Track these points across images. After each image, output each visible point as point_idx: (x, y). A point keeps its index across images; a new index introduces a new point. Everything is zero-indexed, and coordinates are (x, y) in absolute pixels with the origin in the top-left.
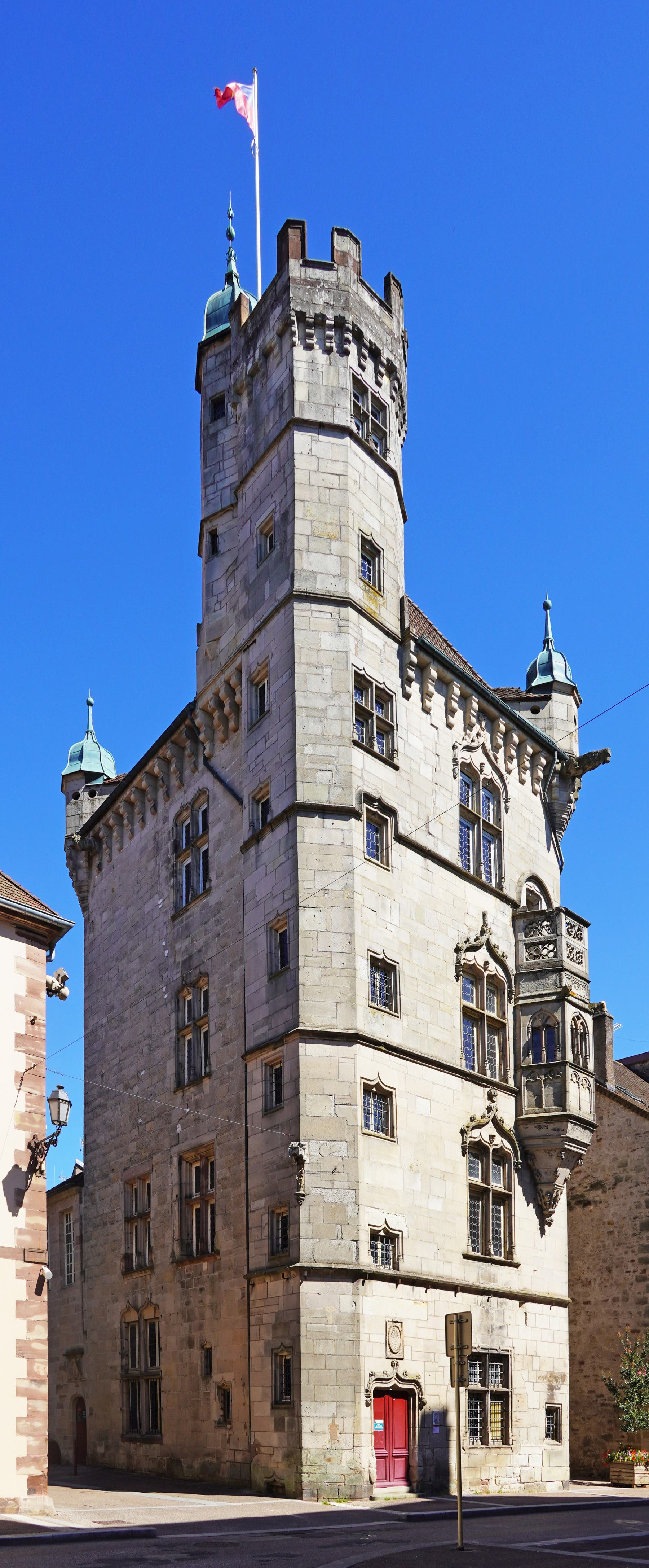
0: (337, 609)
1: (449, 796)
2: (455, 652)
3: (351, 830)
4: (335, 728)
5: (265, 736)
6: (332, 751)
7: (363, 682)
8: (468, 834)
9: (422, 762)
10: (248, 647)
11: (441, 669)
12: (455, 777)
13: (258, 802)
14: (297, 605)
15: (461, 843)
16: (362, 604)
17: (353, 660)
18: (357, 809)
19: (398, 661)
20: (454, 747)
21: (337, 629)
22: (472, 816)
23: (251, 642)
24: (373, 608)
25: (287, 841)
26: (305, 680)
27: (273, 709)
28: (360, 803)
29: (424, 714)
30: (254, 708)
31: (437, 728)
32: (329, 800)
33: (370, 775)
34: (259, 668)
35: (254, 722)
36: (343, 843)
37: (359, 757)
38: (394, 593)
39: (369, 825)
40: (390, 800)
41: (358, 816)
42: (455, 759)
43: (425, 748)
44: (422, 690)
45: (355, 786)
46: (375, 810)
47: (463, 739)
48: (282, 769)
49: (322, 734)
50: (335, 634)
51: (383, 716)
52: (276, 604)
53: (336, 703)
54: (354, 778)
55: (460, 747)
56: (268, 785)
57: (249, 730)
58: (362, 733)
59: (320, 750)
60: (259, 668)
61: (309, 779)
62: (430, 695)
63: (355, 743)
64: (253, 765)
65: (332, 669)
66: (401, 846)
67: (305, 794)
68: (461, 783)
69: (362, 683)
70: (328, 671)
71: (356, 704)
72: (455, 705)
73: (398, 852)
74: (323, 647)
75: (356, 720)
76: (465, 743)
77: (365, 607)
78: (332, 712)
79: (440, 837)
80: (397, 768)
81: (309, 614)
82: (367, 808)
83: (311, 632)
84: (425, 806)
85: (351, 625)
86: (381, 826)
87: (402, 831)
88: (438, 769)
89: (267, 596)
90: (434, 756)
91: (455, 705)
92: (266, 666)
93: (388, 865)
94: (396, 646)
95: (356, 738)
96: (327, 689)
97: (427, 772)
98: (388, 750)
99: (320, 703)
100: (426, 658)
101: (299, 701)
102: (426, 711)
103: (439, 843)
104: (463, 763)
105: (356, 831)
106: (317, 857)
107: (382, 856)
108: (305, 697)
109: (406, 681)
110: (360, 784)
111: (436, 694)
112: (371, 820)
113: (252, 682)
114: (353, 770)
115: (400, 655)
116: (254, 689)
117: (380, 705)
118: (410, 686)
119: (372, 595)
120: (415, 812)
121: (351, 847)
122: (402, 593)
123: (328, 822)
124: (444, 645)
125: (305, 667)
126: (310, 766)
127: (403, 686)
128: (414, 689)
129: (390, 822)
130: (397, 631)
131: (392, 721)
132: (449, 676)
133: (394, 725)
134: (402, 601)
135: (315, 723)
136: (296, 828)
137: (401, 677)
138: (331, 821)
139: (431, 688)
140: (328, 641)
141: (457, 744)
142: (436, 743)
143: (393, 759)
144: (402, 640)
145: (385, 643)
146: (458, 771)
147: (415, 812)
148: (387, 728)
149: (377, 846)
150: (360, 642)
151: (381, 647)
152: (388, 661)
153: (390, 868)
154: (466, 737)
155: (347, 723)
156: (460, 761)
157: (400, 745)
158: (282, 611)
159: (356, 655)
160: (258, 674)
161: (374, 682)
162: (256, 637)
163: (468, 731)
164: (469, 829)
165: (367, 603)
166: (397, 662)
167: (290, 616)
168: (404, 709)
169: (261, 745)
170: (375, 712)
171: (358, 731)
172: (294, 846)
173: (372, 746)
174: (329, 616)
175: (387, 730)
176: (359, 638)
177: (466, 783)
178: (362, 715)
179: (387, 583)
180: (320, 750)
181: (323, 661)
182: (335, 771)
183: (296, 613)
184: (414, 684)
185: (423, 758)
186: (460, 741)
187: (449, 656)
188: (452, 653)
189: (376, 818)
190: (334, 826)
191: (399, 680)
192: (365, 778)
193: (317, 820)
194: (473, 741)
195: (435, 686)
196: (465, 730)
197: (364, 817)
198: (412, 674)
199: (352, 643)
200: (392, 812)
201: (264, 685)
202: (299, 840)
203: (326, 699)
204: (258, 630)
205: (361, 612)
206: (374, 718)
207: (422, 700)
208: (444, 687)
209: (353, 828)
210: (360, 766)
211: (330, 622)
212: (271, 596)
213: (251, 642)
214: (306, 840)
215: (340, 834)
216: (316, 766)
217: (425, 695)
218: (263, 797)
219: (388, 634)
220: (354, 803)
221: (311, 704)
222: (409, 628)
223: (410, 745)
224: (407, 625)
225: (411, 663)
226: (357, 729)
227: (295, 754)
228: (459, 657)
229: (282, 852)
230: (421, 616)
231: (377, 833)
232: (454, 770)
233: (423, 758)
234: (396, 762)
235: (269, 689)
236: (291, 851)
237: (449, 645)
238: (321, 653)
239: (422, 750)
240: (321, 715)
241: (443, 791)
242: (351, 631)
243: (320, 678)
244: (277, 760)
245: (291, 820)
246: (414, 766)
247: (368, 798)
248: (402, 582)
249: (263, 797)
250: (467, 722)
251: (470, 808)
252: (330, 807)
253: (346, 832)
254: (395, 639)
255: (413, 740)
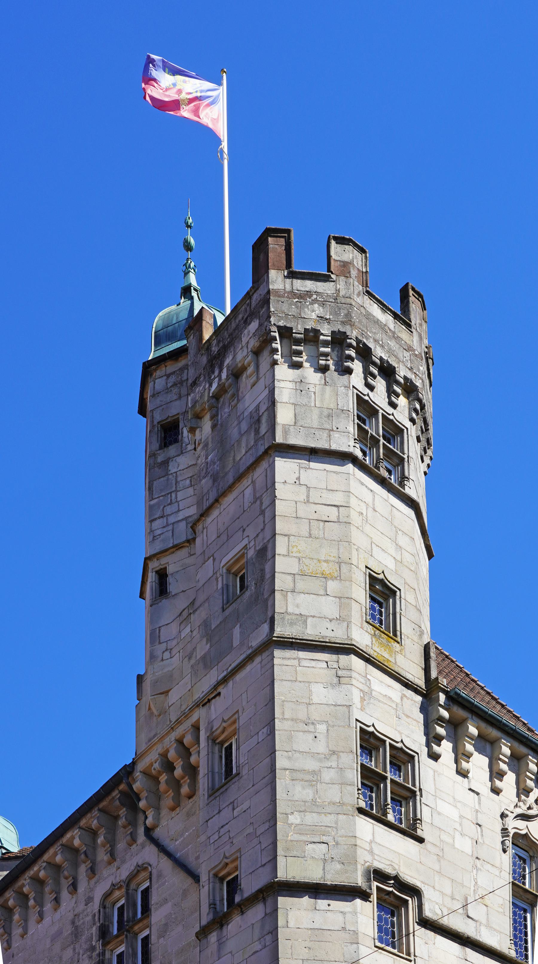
0: (334, 657)
1: (497, 872)
2: (503, 706)
3: (355, 913)
4: (333, 794)
5: (233, 802)
6: (329, 820)
7: (372, 740)
8: (525, 919)
9: (457, 835)
10: (209, 701)
11: (483, 725)
12: (505, 851)
13: (222, 879)
14: (278, 653)
15: (515, 929)
16: (371, 652)
17: (357, 714)
18: (364, 886)
19: (422, 716)
20: (503, 816)
21: (335, 680)
22: (529, 896)
23: (214, 694)
24: (387, 656)
25: (263, 927)
26: (290, 738)
27: (244, 772)
28: (369, 880)
29: (460, 778)
30: (216, 770)
31: (478, 794)
32: (324, 877)
33: (382, 847)
34: (224, 725)
35: (217, 786)
36: (344, 929)
37: (366, 827)
38: (416, 638)
39: (380, 906)
40: (410, 877)
41: (365, 896)
42: (504, 831)
43: (461, 817)
44: (455, 750)
45: (361, 861)
46: (391, 889)
47: (516, 806)
48: (256, 841)
49: (314, 801)
50: (333, 686)
51: (401, 780)
52: (250, 651)
53: (334, 764)
54: (359, 851)
55: (512, 816)
56: (236, 859)
57: (209, 796)
58: (371, 798)
59: (311, 818)
60: (224, 725)
61: (295, 853)
62: (468, 756)
63: (361, 811)
64: (216, 837)
65: (328, 725)
66: (428, 932)
67: (288, 870)
68: (514, 857)
69: (370, 742)
70: (322, 728)
71: (362, 765)
72: (504, 767)
73: (423, 941)
74: (315, 700)
75: (362, 784)
76: (519, 811)
77: (375, 655)
78: (328, 775)
79: (484, 921)
80: (421, 840)
81: (296, 662)
82: (378, 888)
83: (297, 683)
84: (463, 885)
85: (354, 675)
86: (398, 908)
87: (428, 913)
88: (480, 840)
89: (236, 642)
90: (474, 827)
91: (504, 767)
92: (234, 722)
93: (409, 954)
94: (419, 699)
95: (362, 804)
96: (321, 747)
97: (465, 845)
98: (407, 819)
99: (311, 765)
100: (461, 713)
101: (281, 762)
102: (463, 774)
103: (483, 929)
104: (515, 834)
105: (364, 915)
106: (308, 944)
107: (401, 944)
108: (289, 758)
109: (433, 739)
110: (369, 858)
111: (476, 754)
112: (385, 901)
113: (214, 741)
114: (359, 842)
115: (423, 709)
116: (217, 748)
117: (396, 766)
118: (439, 745)
119: (384, 641)
120: (448, 891)
121: (355, 933)
122: (426, 639)
123: (322, 903)
124: (488, 698)
125: (290, 723)
126: (296, 837)
127: (428, 745)
128: (446, 748)
129: (412, 903)
130: (421, 682)
131: (414, 785)
132: (494, 733)
133: (417, 789)
134: (427, 648)
135: (304, 788)
136: (276, 910)
137: (426, 734)
138: (325, 902)
139: (469, 748)
140: (321, 694)
141: (506, 812)
142: (477, 811)
143: (415, 829)
144: (428, 693)
145: (403, 696)
146: (509, 843)
147: (448, 891)
148: (408, 794)
149: (393, 933)
150: (367, 695)
151: (398, 700)
152: (408, 716)
153: (412, 958)
154: (521, 804)
155: (349, 788)
156: (512, 832)
157: (425, 813)
158: (258, 659)
159: (362, 709)
160: (223, 732)
161: (388, 741)
162: (220, 689)
163: (523, 797)
164: (525, 911)
165: (377, 650)
166: (421, 717)
167: (269, 665)
168: (431, 772)
169: (226, 813)
170: (389, 775)
171: (365, 796)
172: (274, 931)
173: (385, 814)
174: (325, 665)
175: (406, 796)
176: (366, 689)
177: (520, 858)
178: (371, 779)
179: (406, 627)
180: (311, 818)
181: (315, 716)
182: (331, 843)
183: (276, 661)
184: (444, 742)
185: (460, 829)
186: (511, 808)
187: (495, 711)
188: (499, 707)
189: (392, 899)
190: (330, 908)
191: (424, 738)
192: (376, 851)
193: (306, 900)
194: (529, 808)
195: (474, 746)
196: (518, 796)
197: (374, 897)
198: (441, 731)
199: (356, 696)
200: (415, 892)
201: (231, 745)
202: (280, 924)
203: (320, 760)
204: (224, 681)
205: (368, 660)
206: (388, 782)
207: (456, 761)
208: (488, 747)
209: (359, 910)
210: (368, 838)
211: (326, 671)
212: (242, 644)
213: (214, 694)
214: (291, 924)
215: (340, 917)
216: (304, 838)
217: (460, 755)
218: (229, 874)
219: (407, 685)
220: (360, 881)
221: (297, 765)
222: (437, 679)
223: (439, 813)
224: (434, 674)
225: (441, 719)
226: (364, 795)
227: (275, 824)
228: (509, 711)
229: (256, 938)
230: (453, 665)
231: (393, 915)
232: (503, 843)
233: (460, 829)
234: (419, 833)
235: (238, 749)
236: (269, 938)
237: (493, 698)
238: (312, 708)
239: (457, 819)
240: (313, 779)
241: (488, 867)
242: (354, 682)
243: (312, 736)
244: (250, 830)
245: (269, 901)
246: (444, 837)
247: (380, 875)
248: (426, 626)
249: (229, 874)
250: (522, 786)
251: (527, 887)
252: (326, 885)
253: (348, 916)
254: (416, 690)
255: (444, 807)
